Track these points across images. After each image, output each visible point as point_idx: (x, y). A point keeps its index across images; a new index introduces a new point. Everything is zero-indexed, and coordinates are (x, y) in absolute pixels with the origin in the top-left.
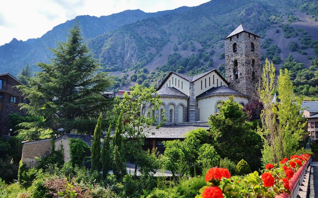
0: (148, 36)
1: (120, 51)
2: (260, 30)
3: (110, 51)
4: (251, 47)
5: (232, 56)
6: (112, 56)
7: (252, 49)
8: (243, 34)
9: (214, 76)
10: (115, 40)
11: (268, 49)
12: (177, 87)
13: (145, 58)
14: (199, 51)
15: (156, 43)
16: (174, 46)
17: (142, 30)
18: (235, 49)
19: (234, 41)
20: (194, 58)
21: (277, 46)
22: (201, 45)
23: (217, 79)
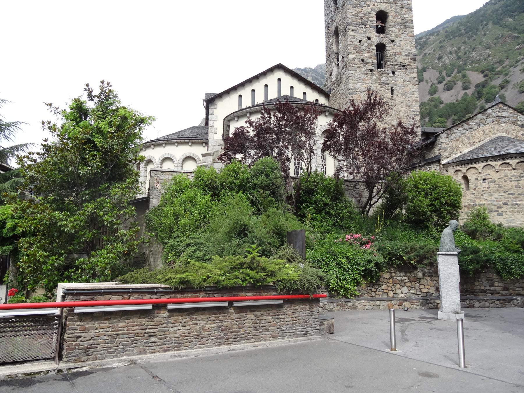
9: (279, 80)
14: (477, 86)
16: (431, 86)
22: (483, 75)
23: (292, 87)
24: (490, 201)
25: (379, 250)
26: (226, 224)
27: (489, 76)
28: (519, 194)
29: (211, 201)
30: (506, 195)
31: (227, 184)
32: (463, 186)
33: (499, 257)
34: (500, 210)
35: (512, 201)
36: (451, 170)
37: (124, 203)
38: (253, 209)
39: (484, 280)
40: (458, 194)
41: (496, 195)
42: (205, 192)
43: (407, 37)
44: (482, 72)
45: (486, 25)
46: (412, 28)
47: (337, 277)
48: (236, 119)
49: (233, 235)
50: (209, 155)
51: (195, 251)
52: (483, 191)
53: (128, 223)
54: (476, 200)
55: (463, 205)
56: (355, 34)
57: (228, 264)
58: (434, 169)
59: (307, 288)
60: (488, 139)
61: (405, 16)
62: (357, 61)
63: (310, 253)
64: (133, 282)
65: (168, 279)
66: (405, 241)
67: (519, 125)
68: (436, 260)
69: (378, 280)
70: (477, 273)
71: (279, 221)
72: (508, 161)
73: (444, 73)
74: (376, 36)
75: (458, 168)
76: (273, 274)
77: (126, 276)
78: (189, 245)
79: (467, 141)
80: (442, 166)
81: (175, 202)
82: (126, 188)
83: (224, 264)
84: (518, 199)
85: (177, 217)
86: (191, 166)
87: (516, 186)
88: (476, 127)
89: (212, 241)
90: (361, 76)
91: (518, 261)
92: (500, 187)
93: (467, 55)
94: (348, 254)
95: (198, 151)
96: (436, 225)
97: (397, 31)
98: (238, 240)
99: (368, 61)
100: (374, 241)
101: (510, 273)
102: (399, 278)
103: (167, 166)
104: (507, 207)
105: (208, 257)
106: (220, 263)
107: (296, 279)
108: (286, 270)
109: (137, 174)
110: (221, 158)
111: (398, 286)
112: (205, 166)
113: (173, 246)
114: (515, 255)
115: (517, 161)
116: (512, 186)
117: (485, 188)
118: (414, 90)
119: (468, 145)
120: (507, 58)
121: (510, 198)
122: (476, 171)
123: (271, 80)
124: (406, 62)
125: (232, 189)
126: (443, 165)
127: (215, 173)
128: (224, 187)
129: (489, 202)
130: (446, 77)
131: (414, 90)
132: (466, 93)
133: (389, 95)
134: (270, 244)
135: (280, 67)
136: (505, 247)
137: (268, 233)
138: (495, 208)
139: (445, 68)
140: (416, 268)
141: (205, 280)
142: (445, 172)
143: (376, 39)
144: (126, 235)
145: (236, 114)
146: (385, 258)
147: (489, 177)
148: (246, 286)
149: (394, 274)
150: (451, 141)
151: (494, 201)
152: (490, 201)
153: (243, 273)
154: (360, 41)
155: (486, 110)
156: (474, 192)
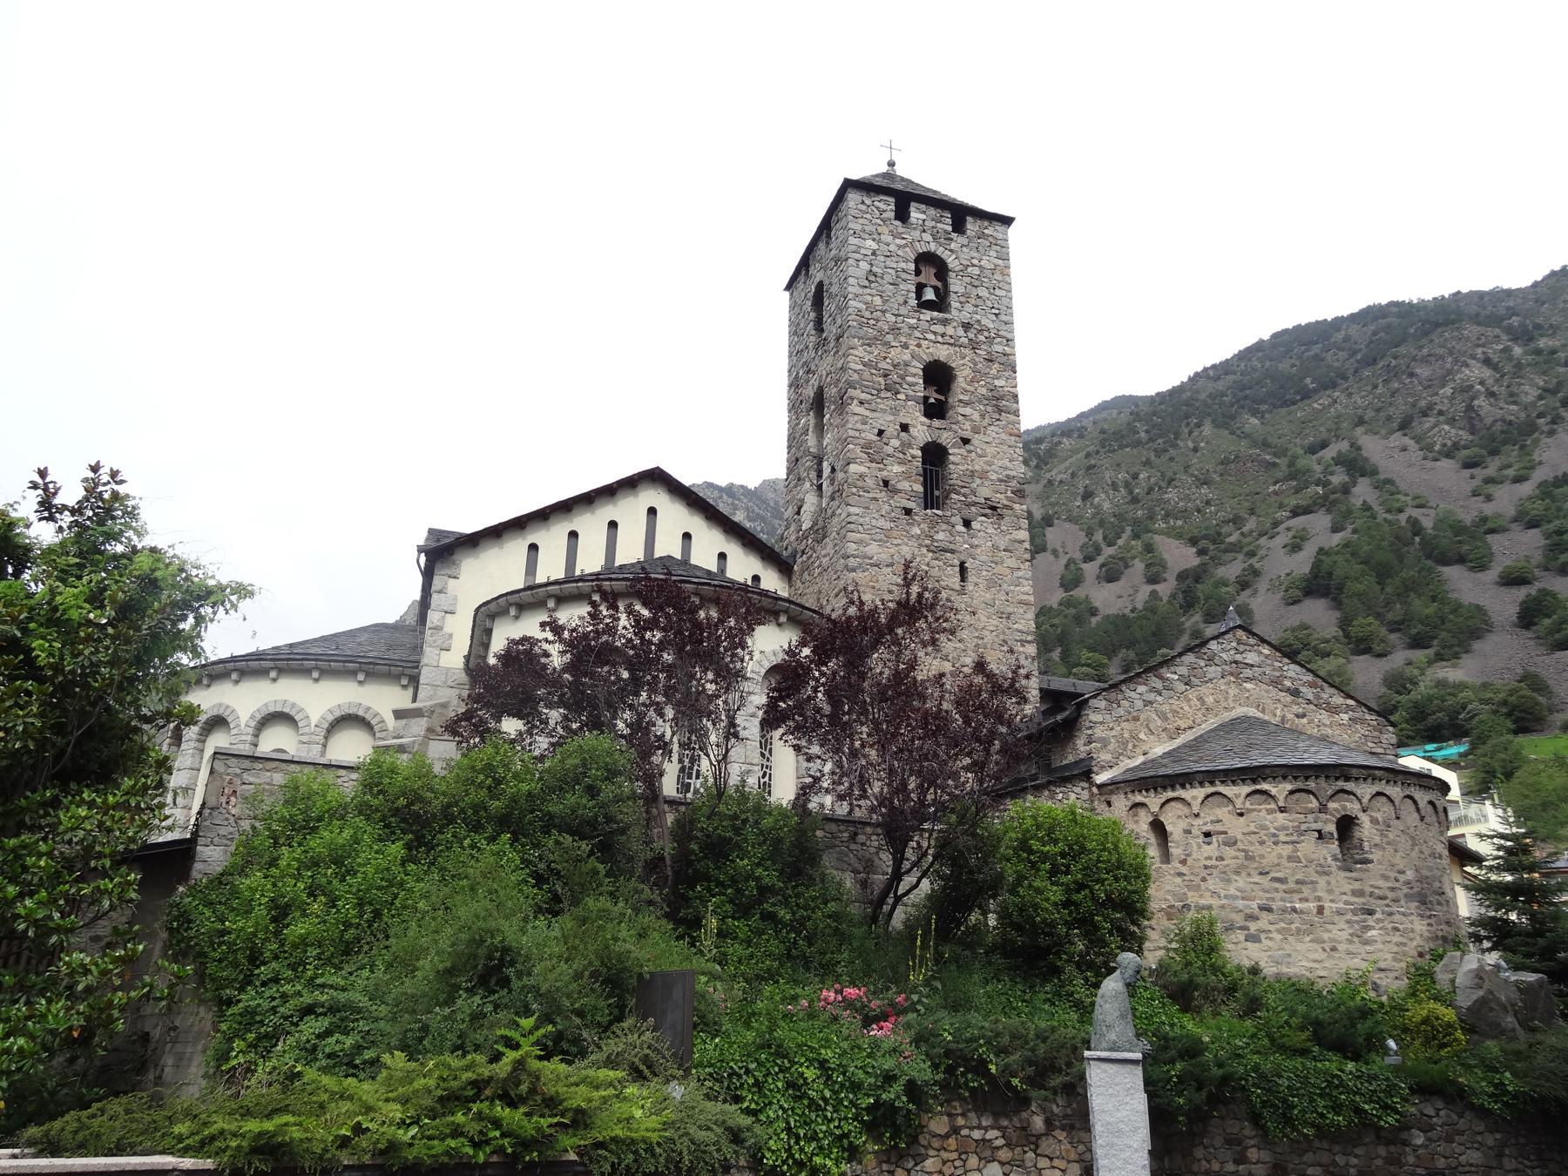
2: (1505, 442)
4: (920, 288)
9: (652, 511)
14: (1182, 576)
16: (1067, 566)
19: (817, 274)
20: (1153, 611)
23: (687, 536)
24: (1226, 897)
25: (918, 1040)
26: (444, 943)
28: (1298, 882)
29: (403, 864)
30: (1264, 881)
31: (462, 811)
32: (1153, 851)
33: (1256, 1068)
34: (1253, 927)
35: (1282, 900)
36: (1121, 803)
37: (100, 856)
38: (540, 896)
39: (1219, 1141)
40: (1140, 873)
41: (1241, 882)
42: (388, 835)
43: (1003, 436)
44: (1193, 541)
45: (1199, 425)
46: (1016, 413)
47: (789, 1129)
48: (513, 612)
49: (462, 981)
50: (417, 713)
51: (328, 1033)
52: (1206, 867)
53: (104, 928)
54: (1190, 894)
55: (1154, 906)
56: (867, 413)
57: (431, 1082)
58: (1073, 797)
59: (690, 1170)
60: (1212, 723)
61: (997, 383)
62: (870, 482)
63: (706, 1047)
64: (81, 1149)
65: (213, 1138)
66: (995, 1014)
67: (1288, 690)
68: (1082, 1077)
69: (914, 1140)
70: (1199, 1117)
71: (616, 939)
72: (1265, 786)
73: (1098, 536)
74: (923, 424)
75: (1139, 798)
76: (580, 1120)
77: (57, 1124)
78: (309, 1010)
79: (1159, 722)
80: (1095, 790)
81: (283, 863)
82: (116, 807)
83: (420, 1083)
84: (1296, 897)
85: (281, 912)
86: (352, 748)
87: (1290, 858)
88: (1181, 687)
89: (390, 999)
90: (881, 523)
91: (1305, 1081)
92: (1249, 858)
93: (1155, 495)
94: (827, 1054)
95: (383, 700)
96: (1083, 965)
97: (976, 416)
98: (477, 1000)
99: (899, 486)
100: (904, 1011)
101: (1288, 1120)
102: (977, 1134)
103: (276, 740)
104: (1271, 917)
105: (368, 1055)
106: (408, 1078)
107: (654, 1137)
108: (625, 1106)
109: (164, 765)
110: (452, 728)
111: (973, 1161)
112: (401, 749)
113: (253, 1013)
114: (1298, 1062)
115: (1289, 787)
116: (1280, 856)
117: (1210, 858)
118: (1020, 574)
119: (1164, 735)
120: (1252, 512)
121: (1277, 890)
122: (1186, 810)
123: (630, 512)
124: (1000, 499)
125: (477, 827)
126: (1099, 787)
127: (430, 771)
128: (450, 820)
129: (1224, 901)
130: (1103, 546)
131: (1020, 574)
132: (1154, 593)
133: (957, 579)
134: (580, 1014)
135: (657, 477)
136: (1272, 1040)
137: (578, 976)
138: (1239, 920)
139: (1102, 523)
140: (1023, 1102)
141: (344, 1142)
142: (1104, 806)
143: (922, 430)
144: (87, 972)
145: (512, 599)
146: (935, 1066)
147: (1219, 827)
148: (486, 1164)
149: (960, 1121)
150: (1118, 720)
151: (1235, 898)
152: (1226, 897)
153: (480, 1116)
154: (881, 433)
155: (1204, 643)
156: (1184, 869)
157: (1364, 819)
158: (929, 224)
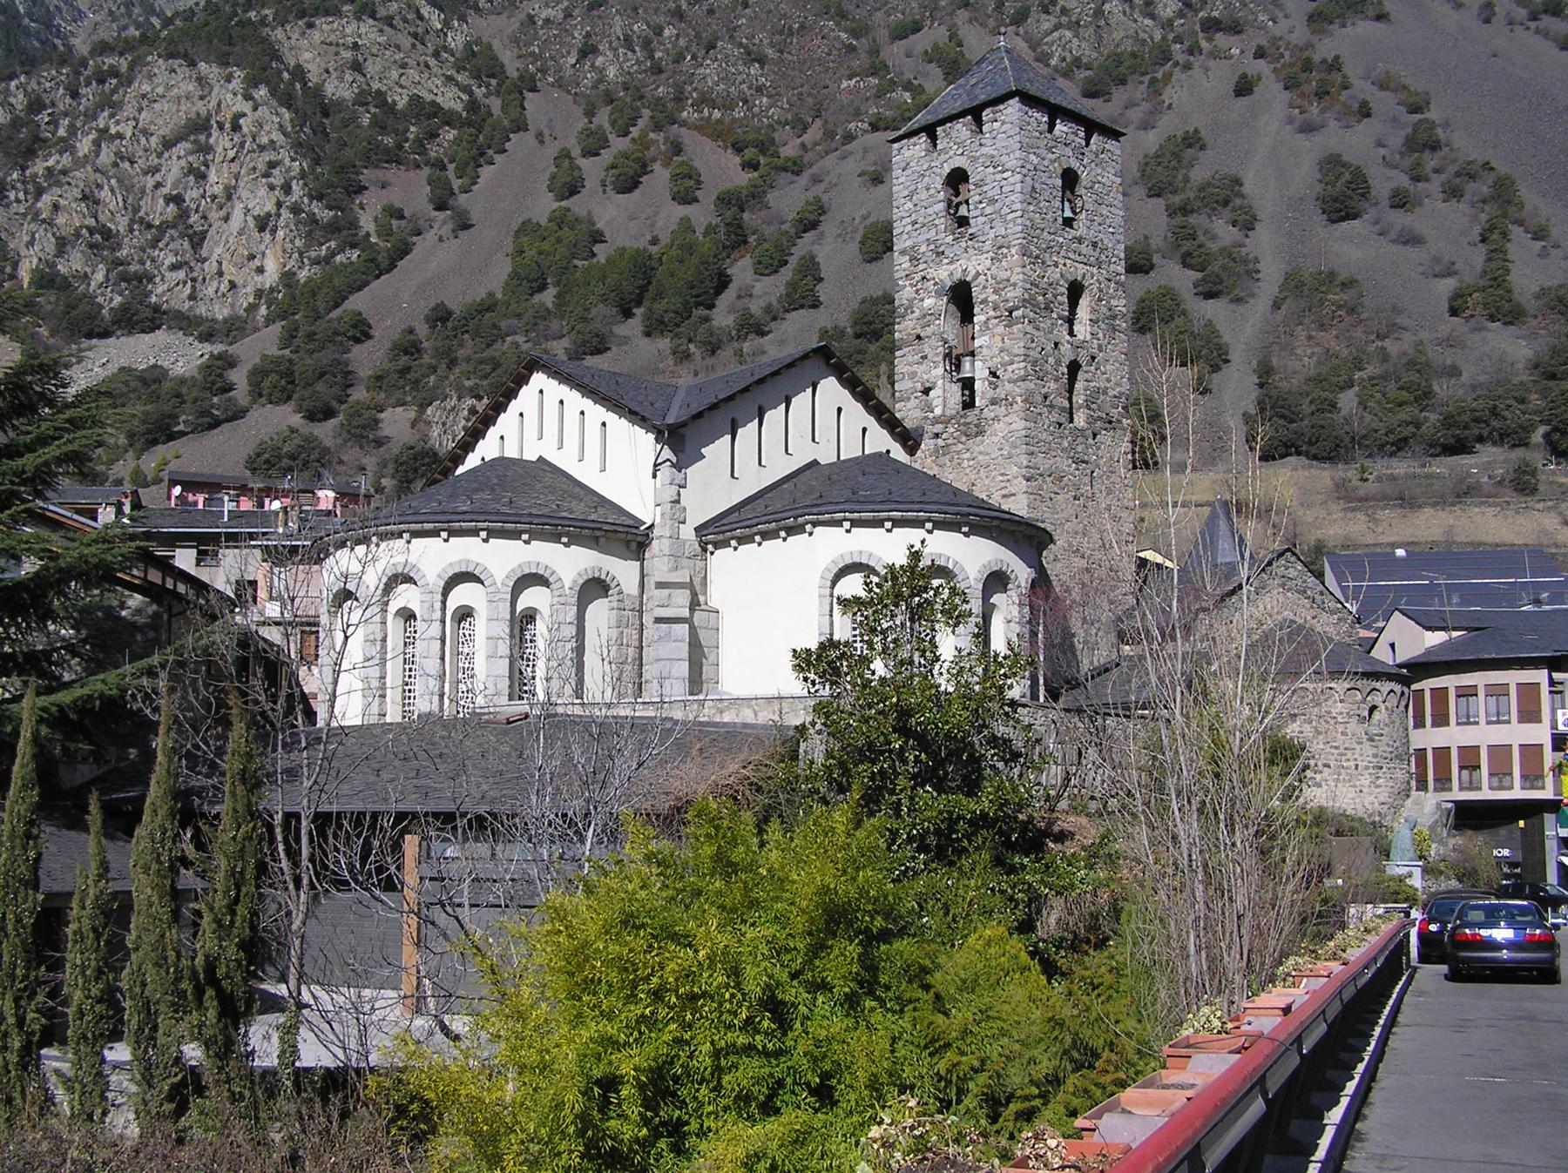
0: (376, 86)
1: (175, 185)
2: (1133, 70)
3: (99, 187)
5: (938, 254)
6: (121, 224)
7: (1068, 214)
8: (1013, 108)
10: (140, 110)
11: (1177, 199)
12: (565, 460)
13: (353, 246)
14: (726, 200)
15: (433, 135)
17: (331, 44)
18: (963, 211)
20: (689, 249)
21: (1237, 182)
22: (738, 160)
27: (762, 170)
139: (610, 99)
157: (1382, 707)
158: (1071, 137)
